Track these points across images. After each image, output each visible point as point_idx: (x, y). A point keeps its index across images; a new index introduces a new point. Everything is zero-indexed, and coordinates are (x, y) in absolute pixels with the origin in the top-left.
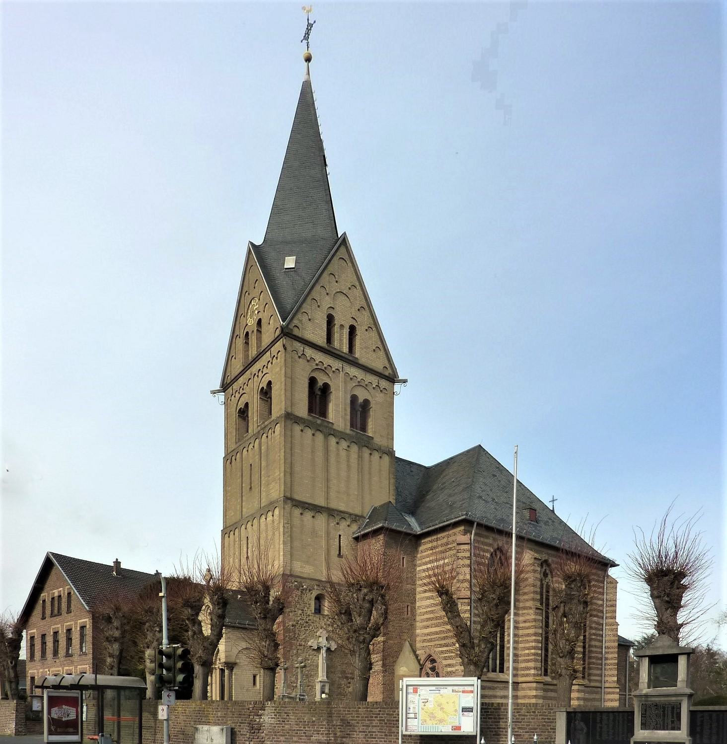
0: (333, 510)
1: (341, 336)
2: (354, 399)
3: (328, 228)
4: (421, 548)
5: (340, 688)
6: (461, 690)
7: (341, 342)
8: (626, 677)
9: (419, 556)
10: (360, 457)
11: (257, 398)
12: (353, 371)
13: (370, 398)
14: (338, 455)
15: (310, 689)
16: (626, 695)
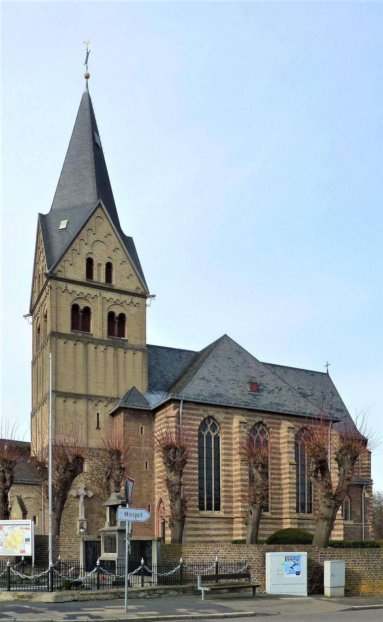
0: (92, 396)
1: (99, 271)
3: (93, 196)
4: (156, 420)
5: (98, 524)
6: (25, 528)
7: (99, 276)
8: (362, 510)
9: (155, 425)
10: (116, 356)
12: (109, 295)
13: (125, 312)
14: (96, 356)
15: (72, 526)
16: (362, 525)
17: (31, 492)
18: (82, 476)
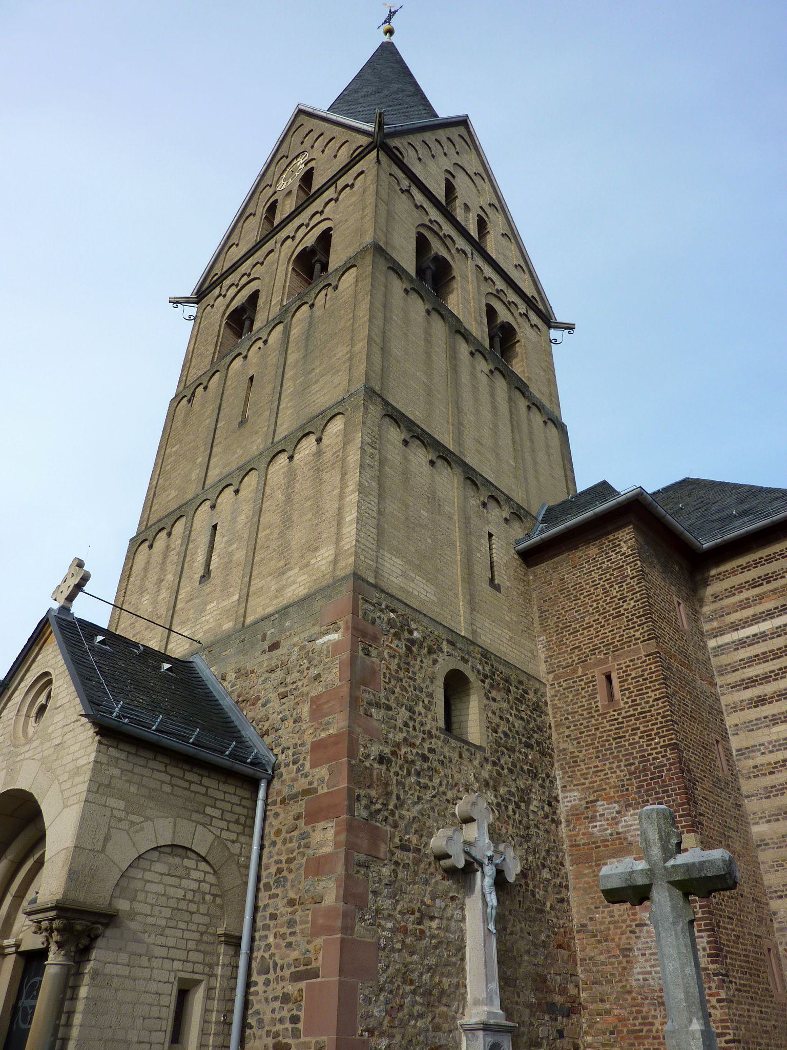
2: (491, 312)
9: (707, 609)
11: (287, 269)
17: (195, 816)
18: (469, 765)
